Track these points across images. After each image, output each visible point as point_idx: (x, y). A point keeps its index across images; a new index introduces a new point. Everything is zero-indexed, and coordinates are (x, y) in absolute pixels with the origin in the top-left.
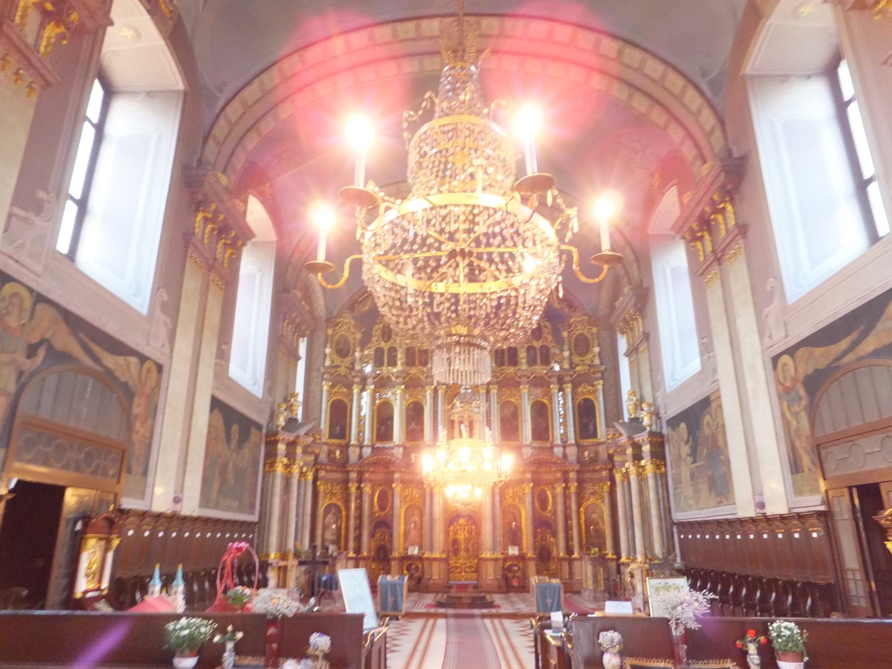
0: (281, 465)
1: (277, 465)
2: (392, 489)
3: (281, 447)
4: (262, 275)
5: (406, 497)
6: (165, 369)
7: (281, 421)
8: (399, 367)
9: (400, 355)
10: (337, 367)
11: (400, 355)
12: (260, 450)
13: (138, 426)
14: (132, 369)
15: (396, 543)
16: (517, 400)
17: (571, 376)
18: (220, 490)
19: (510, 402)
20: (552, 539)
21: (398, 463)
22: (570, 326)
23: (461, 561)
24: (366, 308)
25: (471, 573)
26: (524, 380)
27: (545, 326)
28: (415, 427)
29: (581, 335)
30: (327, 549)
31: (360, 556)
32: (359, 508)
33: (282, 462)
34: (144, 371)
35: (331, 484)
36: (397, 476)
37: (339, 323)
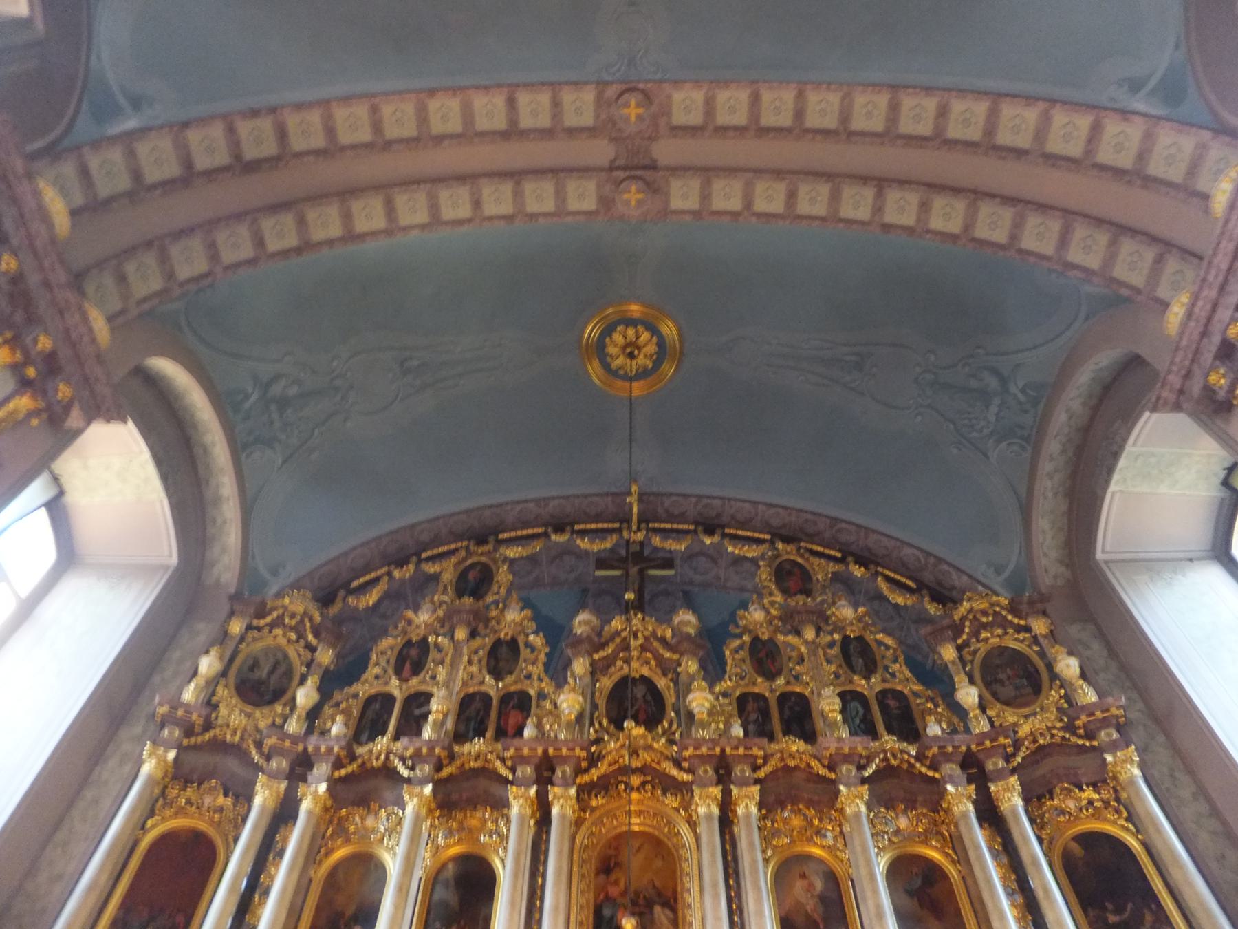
16: (829, 849)
19: (809, 858)
26: (847, 770)
27: (880, 643)
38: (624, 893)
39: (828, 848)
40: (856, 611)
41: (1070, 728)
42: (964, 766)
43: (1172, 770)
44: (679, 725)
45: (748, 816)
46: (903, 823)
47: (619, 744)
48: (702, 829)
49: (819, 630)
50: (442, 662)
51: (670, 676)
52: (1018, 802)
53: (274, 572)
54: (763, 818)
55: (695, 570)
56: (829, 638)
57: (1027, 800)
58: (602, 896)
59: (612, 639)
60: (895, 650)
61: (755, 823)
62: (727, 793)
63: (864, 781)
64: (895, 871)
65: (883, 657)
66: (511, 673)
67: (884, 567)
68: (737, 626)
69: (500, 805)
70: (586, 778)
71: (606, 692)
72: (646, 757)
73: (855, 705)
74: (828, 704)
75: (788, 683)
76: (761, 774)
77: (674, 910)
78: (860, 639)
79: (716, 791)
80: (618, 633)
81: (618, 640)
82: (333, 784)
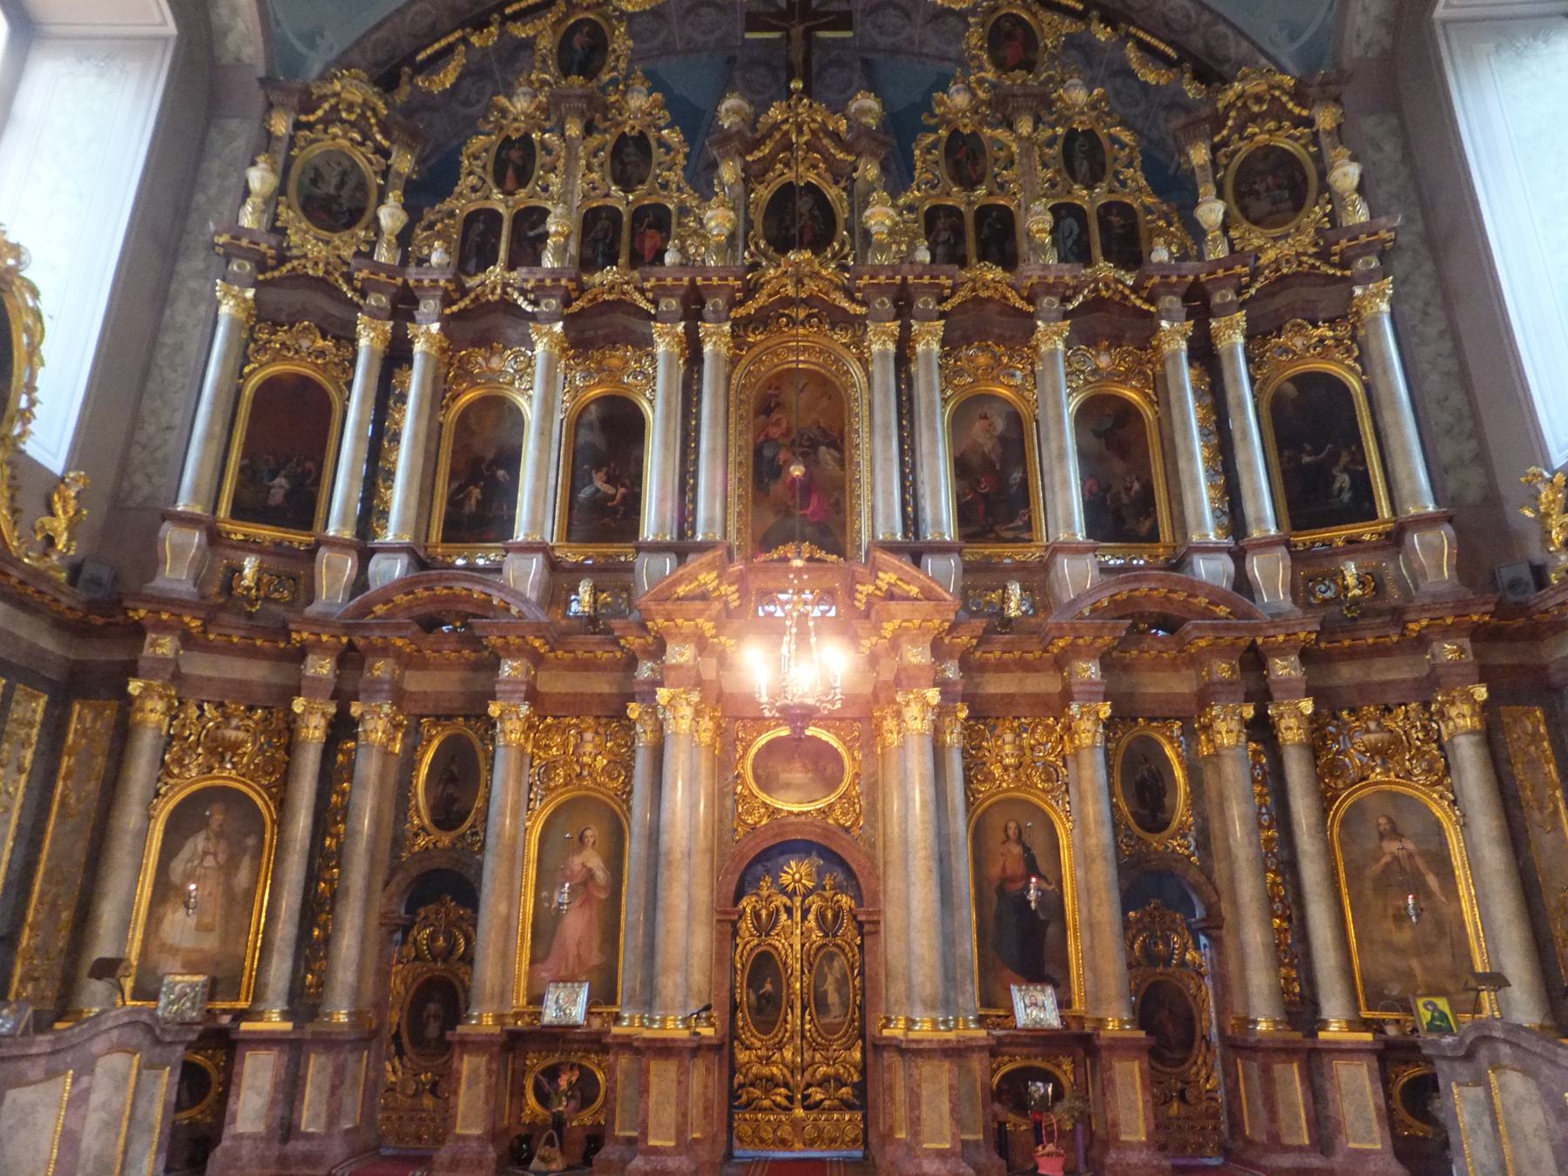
5: (550, 767)
15: (487, 972)
16: (1016, 389)
19: (993, 398)
25: (832, 1109)
26: (1049, 302)
27: (1114, 139)
40: (1090, 93)
41: (1324, 255)
42: (1186, 299)
43: (1427, 304)
44: (852, 248)
45: (928, 353)
46: (1104, 361)
47: (780, 271)
48: (875, 368)
49: (1037, 121)
51: (842, 184)
52: (1239, 340)
54: (945, 355)
55: (881, 28)
56: (1049, 132)
57: (1249, 337)
58: (762, 438)
59: (768, 135)
60: (1132, 149)
61: (935, 361)
62: (905, 328)
63: (1066, 315)
64: (1084, 414)
65: (1116, 159)
67: (1139, 27)
68: (934, 116)
69: (644, 343)
70: (741, 312)
71: (763, 205)
72: (812, 286)
73: (1070, 224)
75: (990, 194)
76: (947, 307)
77: (841, 450)
78: (1090, 134)
79: (894, 327)
80: (776, 126)
81: (778, 136)
82: (446, 321)
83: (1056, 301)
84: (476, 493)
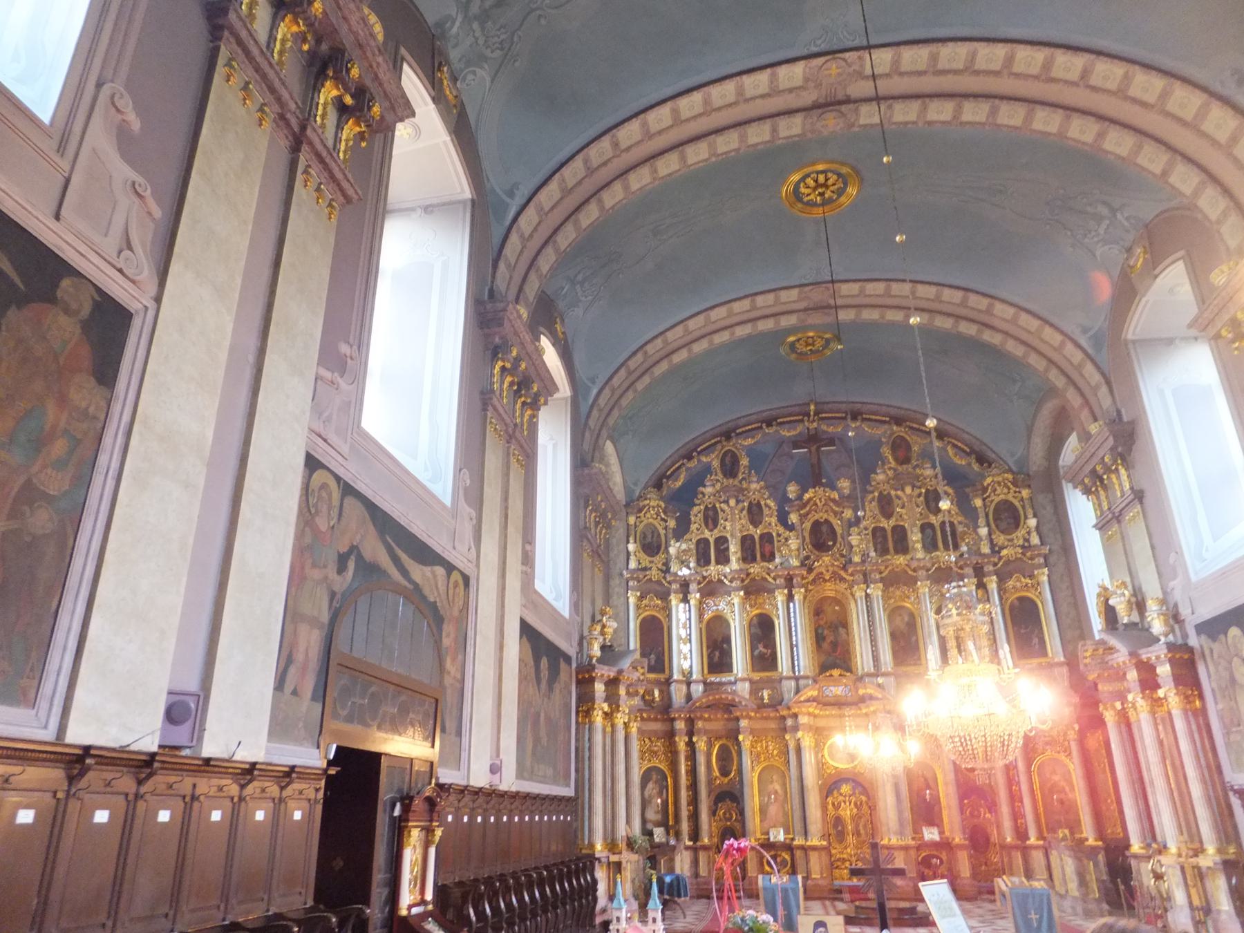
0: (600, 713)
1: (595, 713)
2: (739, 744)
3: (599, 688)
4: (555, 446)
5: (758, 755)
6: (472, 582)
7: (596, 651)
8: (734, 564)
9: (734, 548)
10: (645, 569)
11: (734, 548)
12: (570, 693)
13: (448, 664)
14: (440, 584)
17: (995, 565)
18: (534, 754)
19: (903, 607)
20: (988, 815)
21: (746, 705)
22: (985, 490)
23: (849, 850)
24: (679, 484)
26: (922, 573)
28: (764, 651)
29: (1006, 502)
30: (650, 834)
31: (699, 844)
32: (693, 772)
33: (602, 709)
34: (451, 585)
35: (650, 739)
36: (744, 723)
37: (645, 506)
38: (826, 623)
39: (911, 603)
49: (913, 487)
50: (726, 520)
53: (635, 484)
66: (761, 523)
73: (929, 531)
74: (915, 537)
75: (897, 520)
76: (883, 575)
80: (810, 499)
83: (925, 573)
84: (717, 654)
